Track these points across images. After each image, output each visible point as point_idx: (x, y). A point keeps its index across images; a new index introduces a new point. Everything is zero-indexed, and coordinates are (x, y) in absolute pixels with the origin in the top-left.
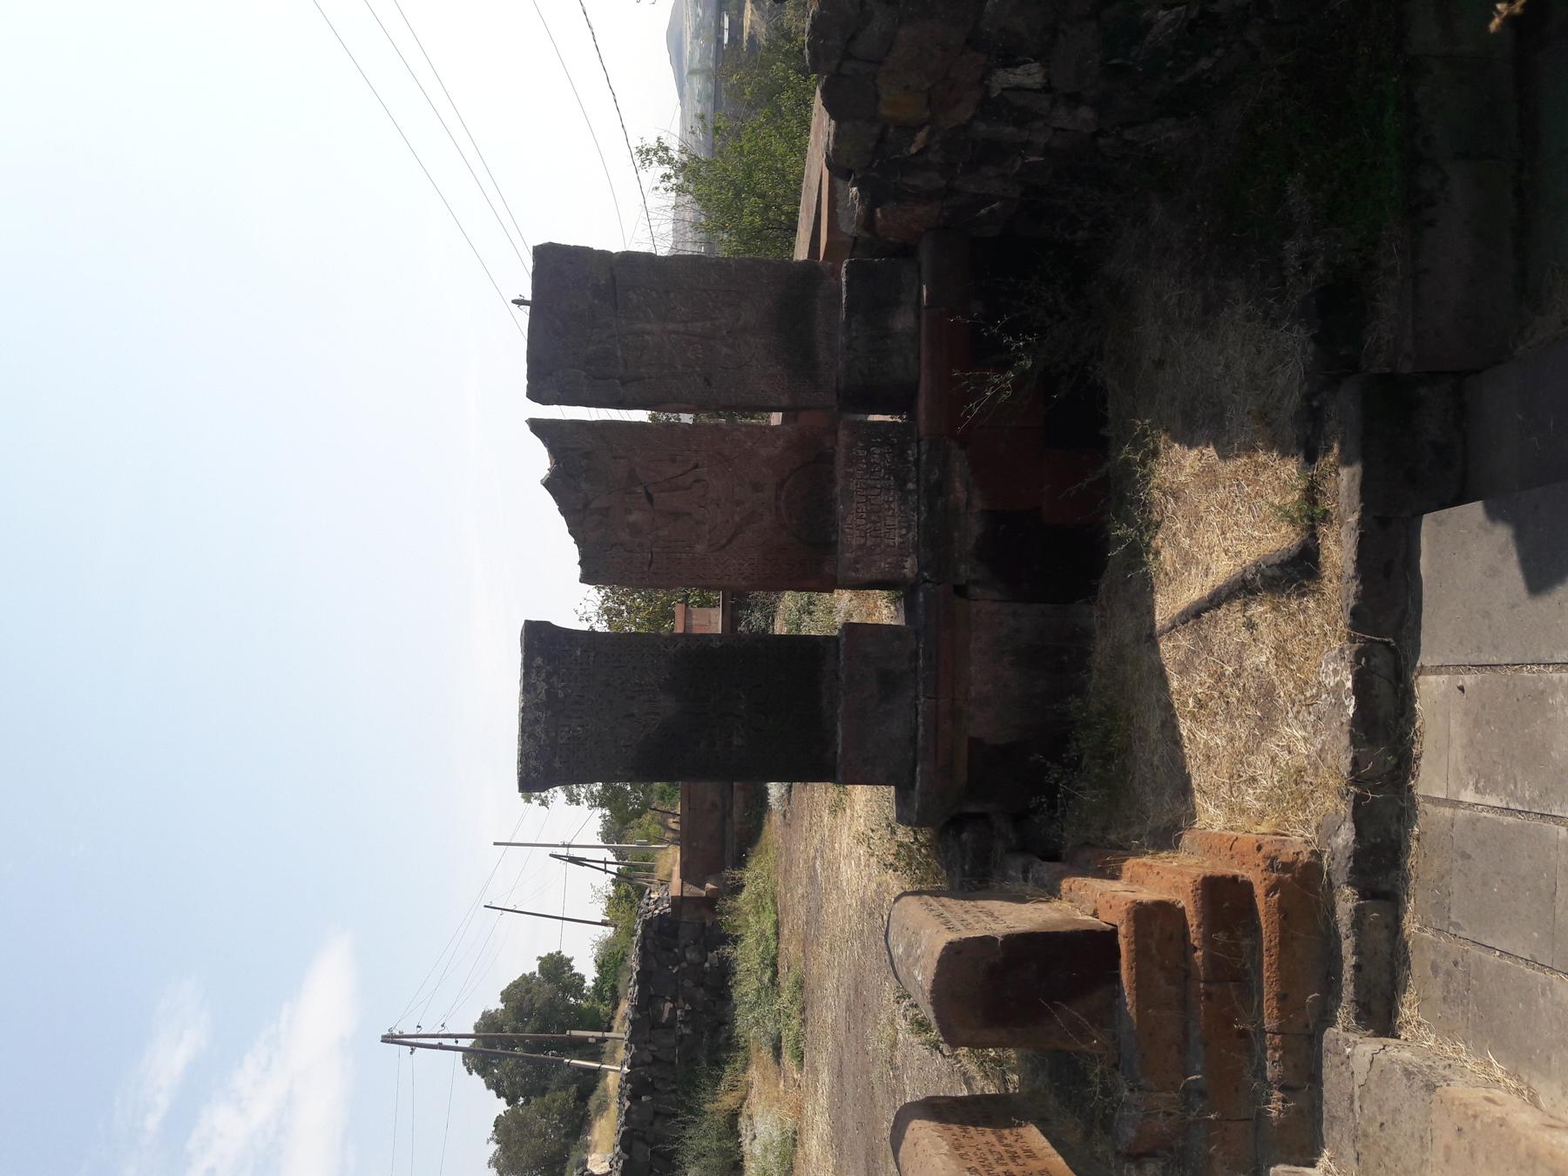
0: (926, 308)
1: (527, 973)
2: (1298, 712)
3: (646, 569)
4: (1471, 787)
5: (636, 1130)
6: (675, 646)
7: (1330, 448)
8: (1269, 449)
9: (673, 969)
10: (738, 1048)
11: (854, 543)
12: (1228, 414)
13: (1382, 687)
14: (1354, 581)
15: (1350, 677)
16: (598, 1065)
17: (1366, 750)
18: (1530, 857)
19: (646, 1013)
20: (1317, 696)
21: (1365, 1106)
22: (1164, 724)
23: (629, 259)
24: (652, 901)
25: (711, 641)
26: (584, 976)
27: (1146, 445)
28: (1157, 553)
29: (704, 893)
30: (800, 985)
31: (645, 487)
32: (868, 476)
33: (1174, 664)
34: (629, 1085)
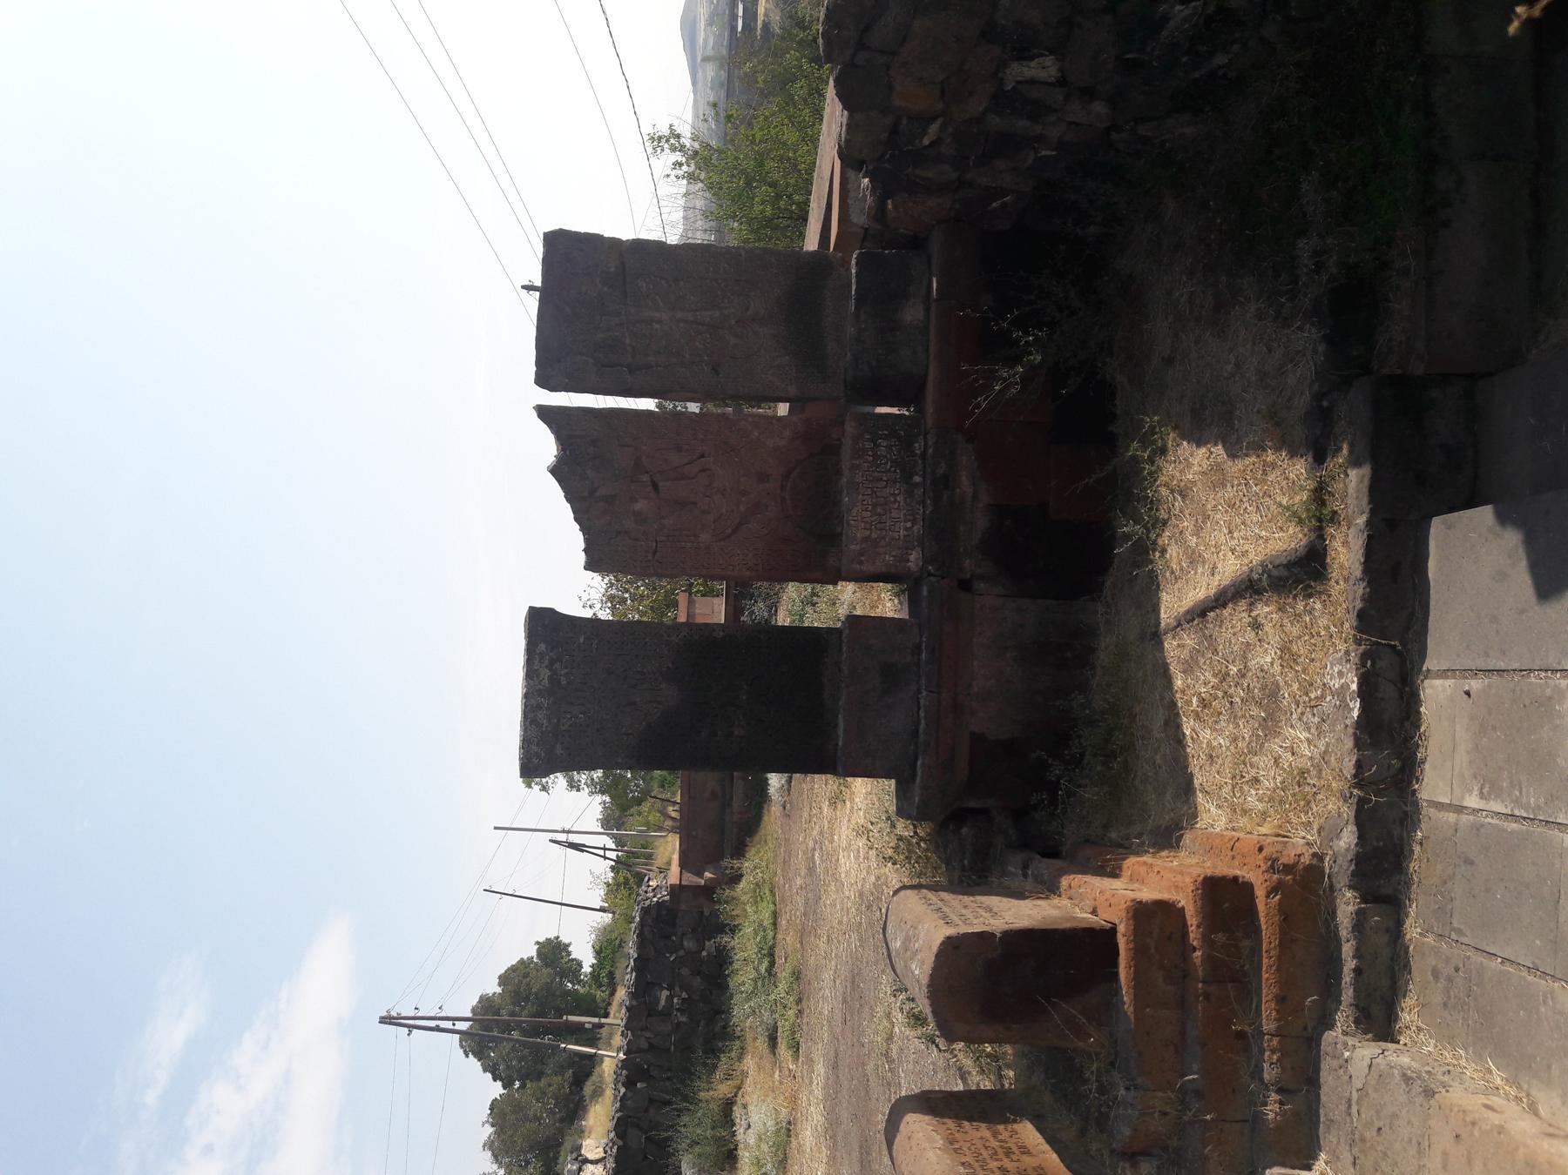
0: (937, 300)
1: (525, 958)
2: (1302, 714)
3: (650, 557)
4: (1476, 792)
5: (630, 1117)
7: (1339, 449)
8: (1277, 449)
9: (671, 956)
10: (733, 1037)
12: (1238, 413)
13: (1388, 691)
14: (1361, 582)
15: (1355, 679)
16: (594, 1051)
18: (1533, 863)
20: (1323, 697)
21: (1362, 1110)
22: (1167, 723)
23: (639, 246)
25: (714, 630)
28: (1164, 551)
29: (703, 882)
30: (797, 976)
31: (651, 476)
33: (1178, 662)
34: (624, 1072)
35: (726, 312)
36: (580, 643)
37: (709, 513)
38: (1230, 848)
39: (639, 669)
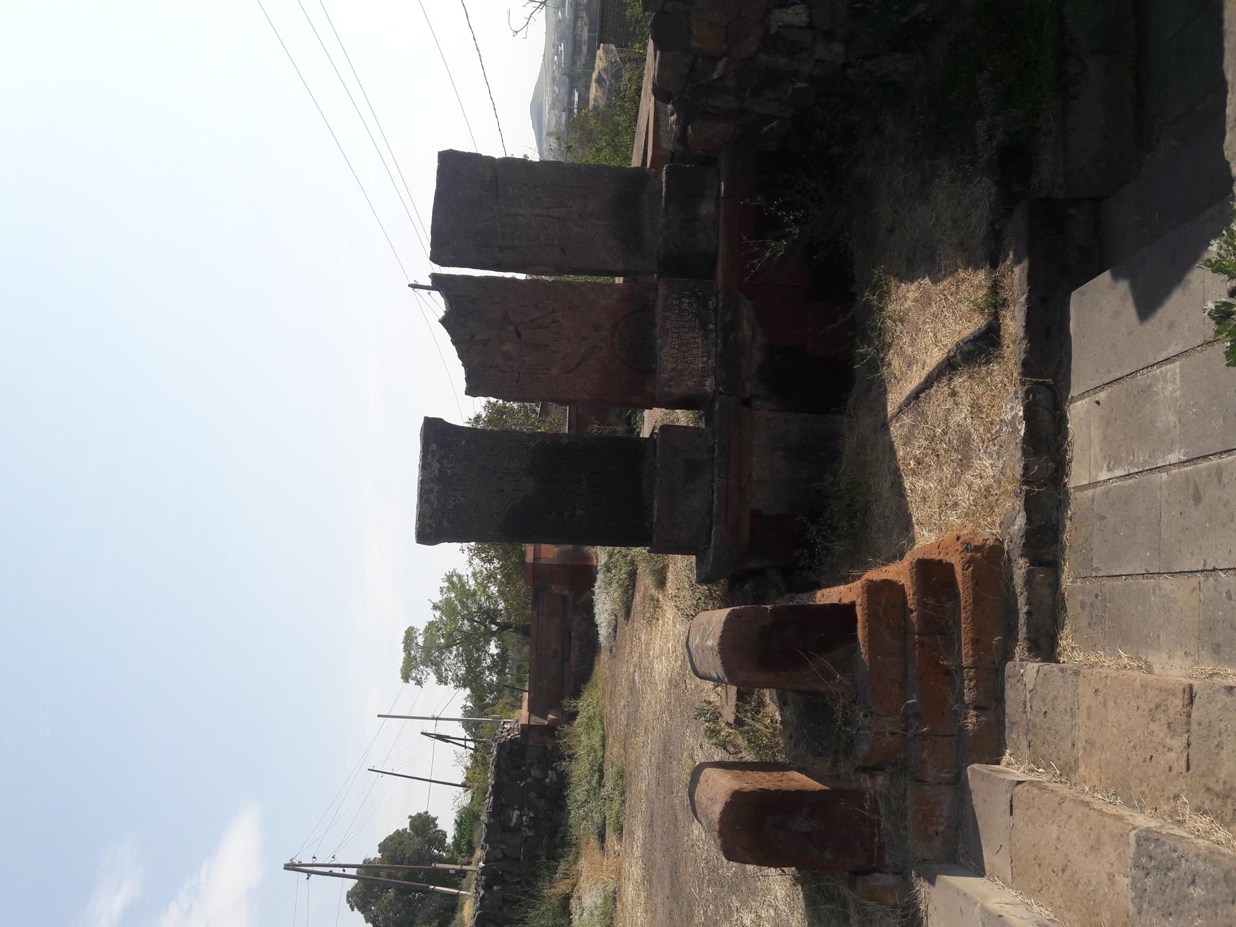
0: (724, 198)
1: (400, 830)
2: (987, 447)
3: (515, 385)
4: (1105, 468)
5: (488, 914)
6: (535, 441)
7: (1009, 255)
8: (966, 268)
10: (570, 845)
11: (668, 366)
13: (1044, 415)
14: (1024, 341)
15: (1022, 408)
16: (457, 891)
17: (1033, 459)
18: (1143, 501)
20: (1000, 429)
21: (1033, 705)
22: (893, 484)
23: (508, 163)
25: (562, 438)
26: (446, 832)
27: (881, 286)
28: (890, 364)
30: (621, 775)
32: (679, 319)
38: (937, 546)
39: (506, 466)
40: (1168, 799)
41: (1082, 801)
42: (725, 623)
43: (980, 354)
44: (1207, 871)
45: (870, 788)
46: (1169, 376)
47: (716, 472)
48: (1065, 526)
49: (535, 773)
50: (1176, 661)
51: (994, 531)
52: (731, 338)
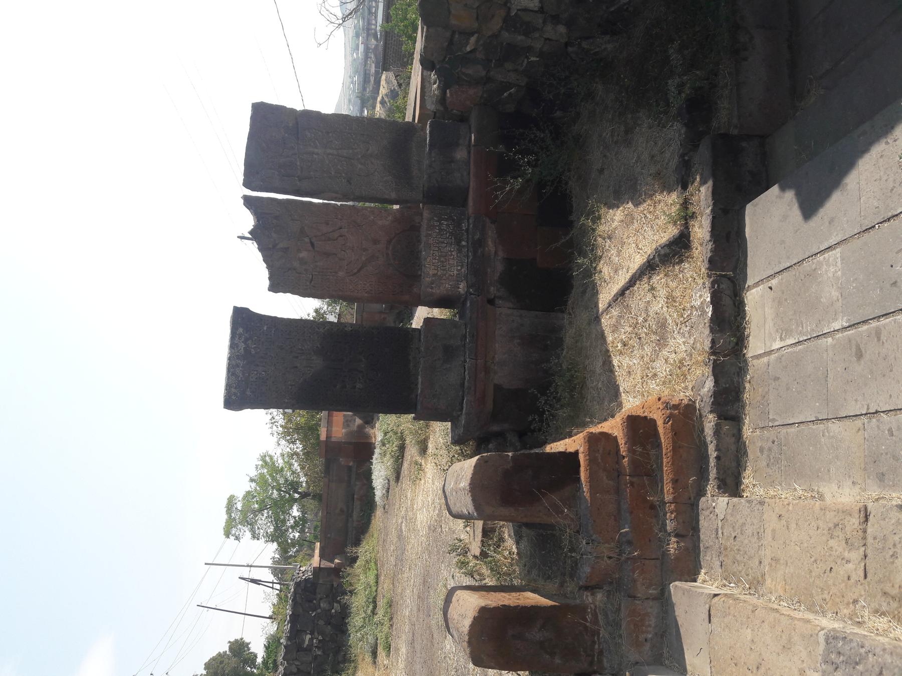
0: (474, 146)
2: (680, 329)
3: (308, 283)
4: (778, 339)
6: (324, 328)
7: (696, 179)
8: (662, 192)
9: (312, 613)
10: (350, 661)
12: (639, 182)
13: (727, 301)
15: (709, 295)
19: (294, 641)
21: (725, 531)
22: (604, 363)
24: (301, 572)
25: (346, 326)
27: (593, 212)
29: (333, 566)
30: (390, 604)
31: (310, 239)
35: (356, 151)
36: (264, 330)
37: (344, 260)
38: (641, 407)
39: (300, 347)
40: (848, 604)
41: (771, 608)
42: (475, 467)
43: (674, 256)
44: (894, 663)
45: (591, 604)
46: (831, 261)
47: (467, 354)
48: (745, 388)
49: (323, 605)
50: (844, 490)
51: (687, 394)
52: (480, 251)
